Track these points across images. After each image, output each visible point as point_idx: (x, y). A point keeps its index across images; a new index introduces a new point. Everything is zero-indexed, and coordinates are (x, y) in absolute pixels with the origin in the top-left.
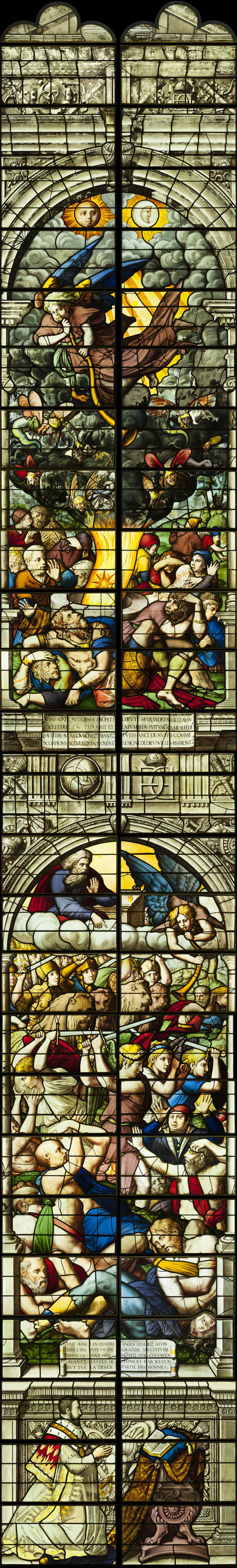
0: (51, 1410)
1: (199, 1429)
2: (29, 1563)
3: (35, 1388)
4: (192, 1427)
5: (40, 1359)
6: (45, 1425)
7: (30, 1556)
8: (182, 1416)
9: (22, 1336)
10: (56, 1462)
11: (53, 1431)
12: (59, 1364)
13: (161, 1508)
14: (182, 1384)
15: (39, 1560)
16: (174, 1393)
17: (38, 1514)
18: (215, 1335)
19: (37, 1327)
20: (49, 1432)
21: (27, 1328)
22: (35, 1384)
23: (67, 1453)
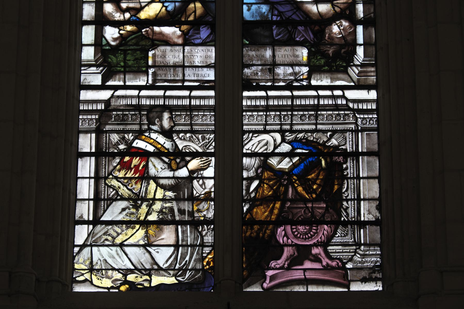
0: (138, 121)
1: (334, 142)
2: (106, 290)
3: (119, 97)
4: (325, 140)
5: (124, 67)
6: (130, 137)
7: (107, 283)
8: (314, 127)
9: (104, 42)
10: (145, 177)
11: (139, 144)
12: (147, 73)
13: (288, 228)
14: (313, 93)
15: (118, 288)
16: (303, 103)
17: (118, 234)
18: (355, 39)
19: (121, 32)
20: (134, 145)
21: (111, 33)
22: (120, 93)
23: (157, 167)
